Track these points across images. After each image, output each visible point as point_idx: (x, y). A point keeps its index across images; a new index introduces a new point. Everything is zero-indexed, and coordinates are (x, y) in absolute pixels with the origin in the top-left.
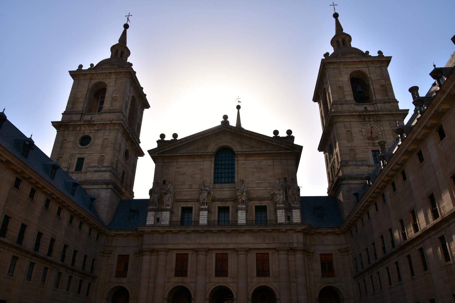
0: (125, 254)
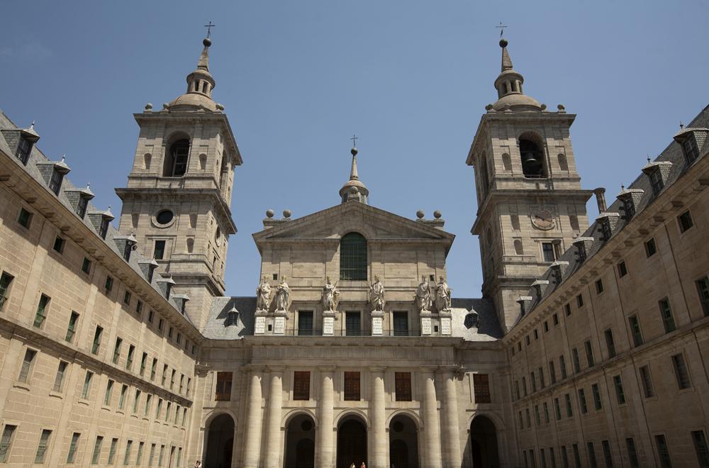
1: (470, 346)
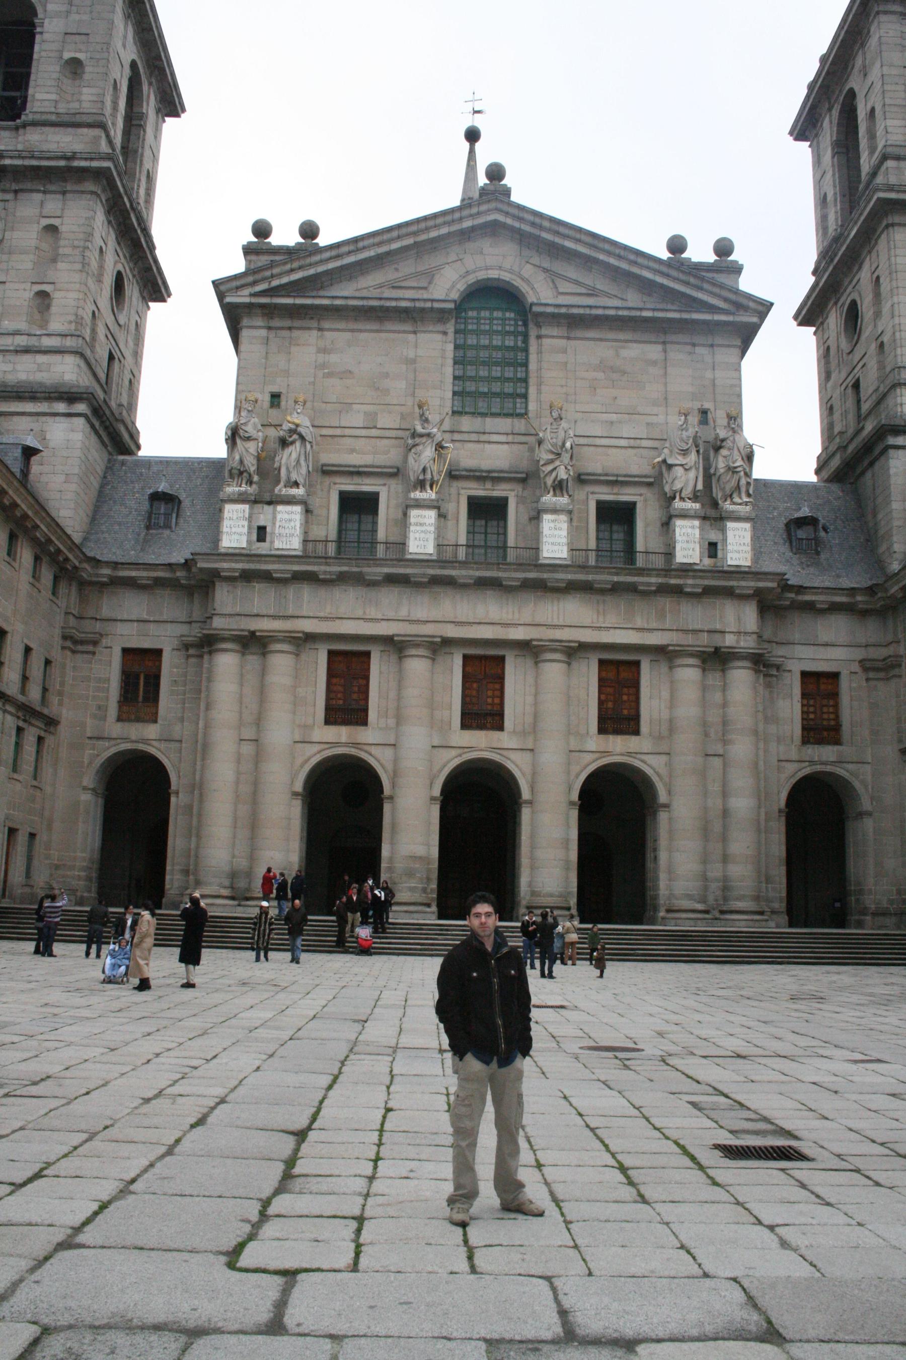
0: (146, 644)
1: (800, 598)
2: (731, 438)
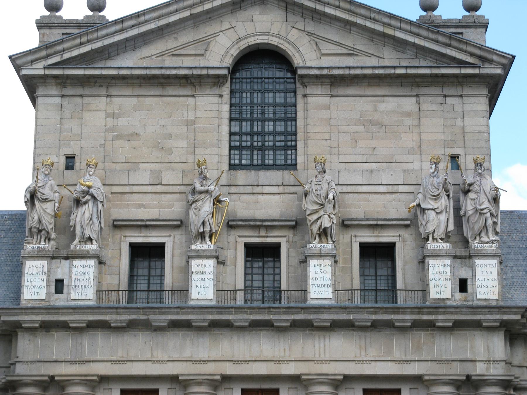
2: (478, 183)
